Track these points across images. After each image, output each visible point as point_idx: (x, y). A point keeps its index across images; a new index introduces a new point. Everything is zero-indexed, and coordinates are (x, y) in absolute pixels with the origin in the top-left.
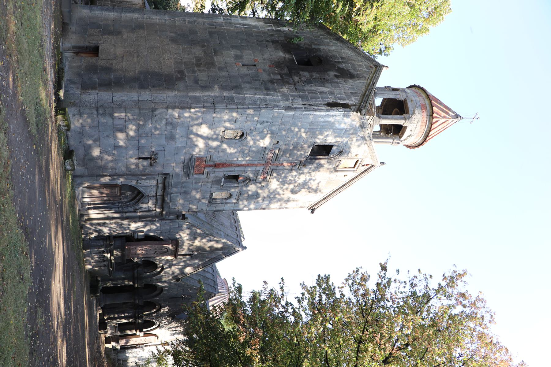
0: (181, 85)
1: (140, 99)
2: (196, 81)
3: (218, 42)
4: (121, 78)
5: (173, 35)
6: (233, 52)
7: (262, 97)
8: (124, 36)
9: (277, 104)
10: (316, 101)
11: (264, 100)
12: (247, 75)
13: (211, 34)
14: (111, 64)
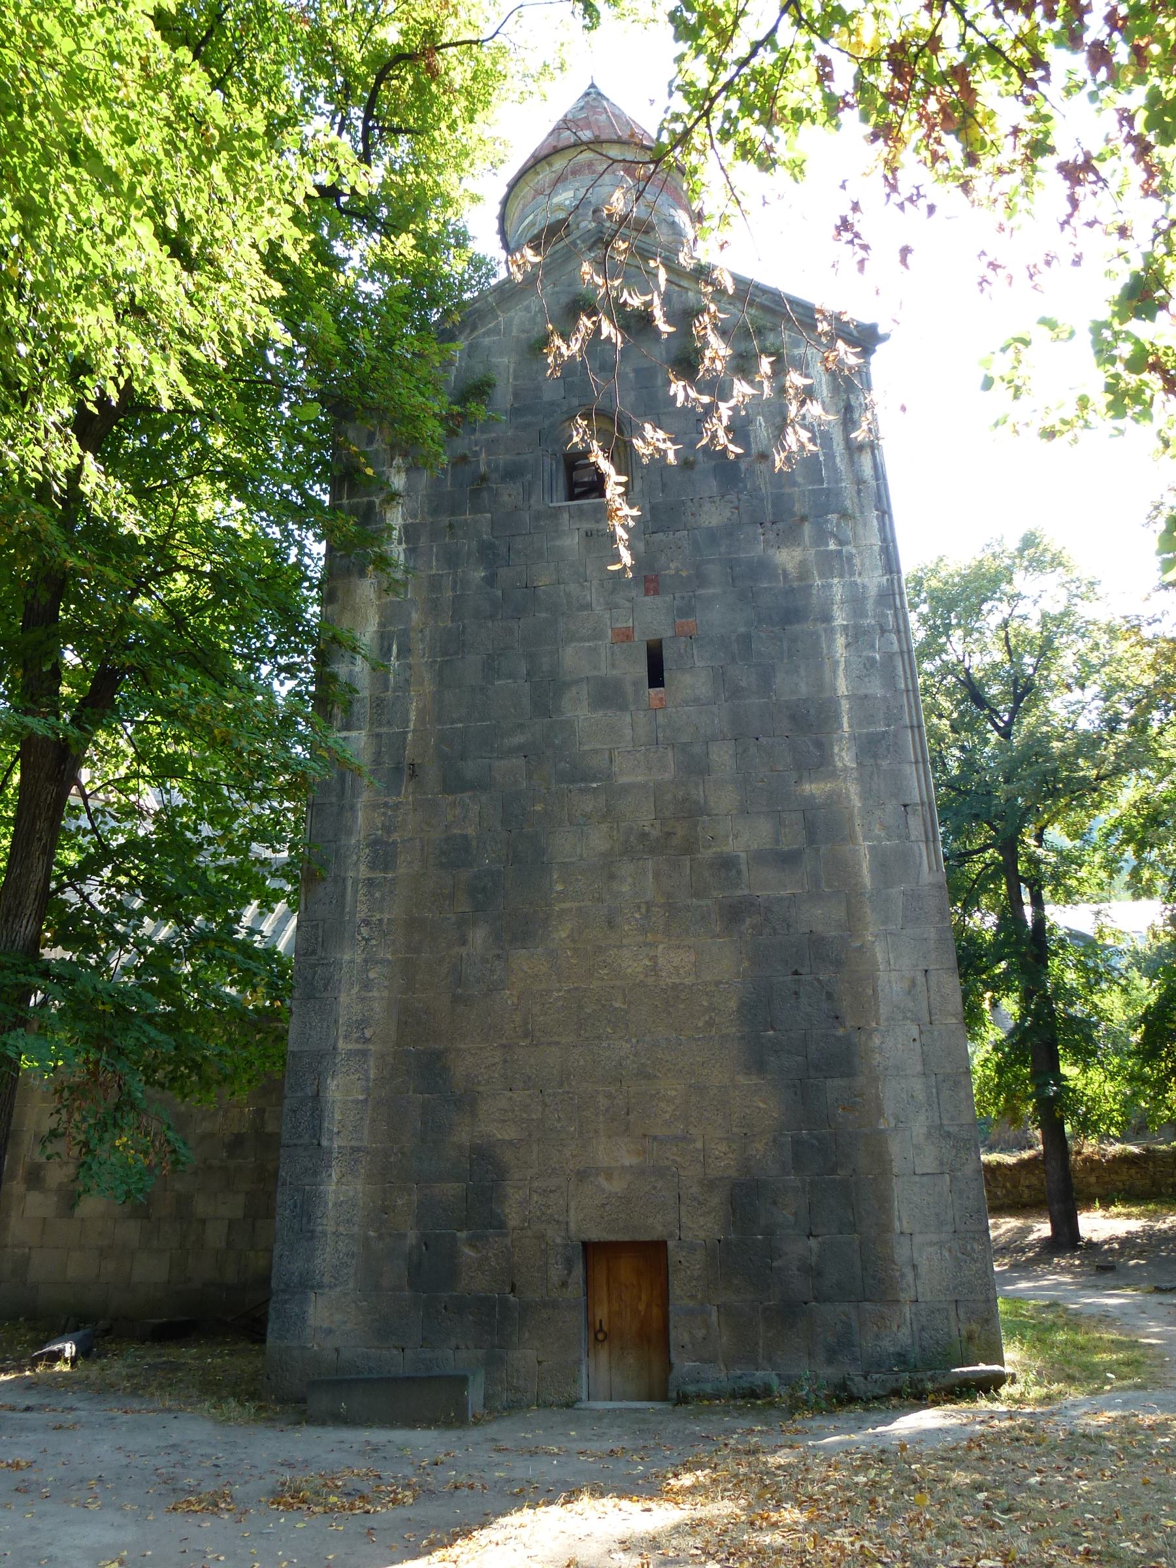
0: (820, 917)
1: (919, 1068)
2: (787, 859)
3: (519, 762)
4: (797, 1142)
5: (479, 936)
6: (578, 711)
7: (840, 641)
8: (509, 1133)
9: (873, 591)
10: (835, 469)
11: (857, 636)
12: (720, 677)
13: (454, 783)
14: (710, 1185)
